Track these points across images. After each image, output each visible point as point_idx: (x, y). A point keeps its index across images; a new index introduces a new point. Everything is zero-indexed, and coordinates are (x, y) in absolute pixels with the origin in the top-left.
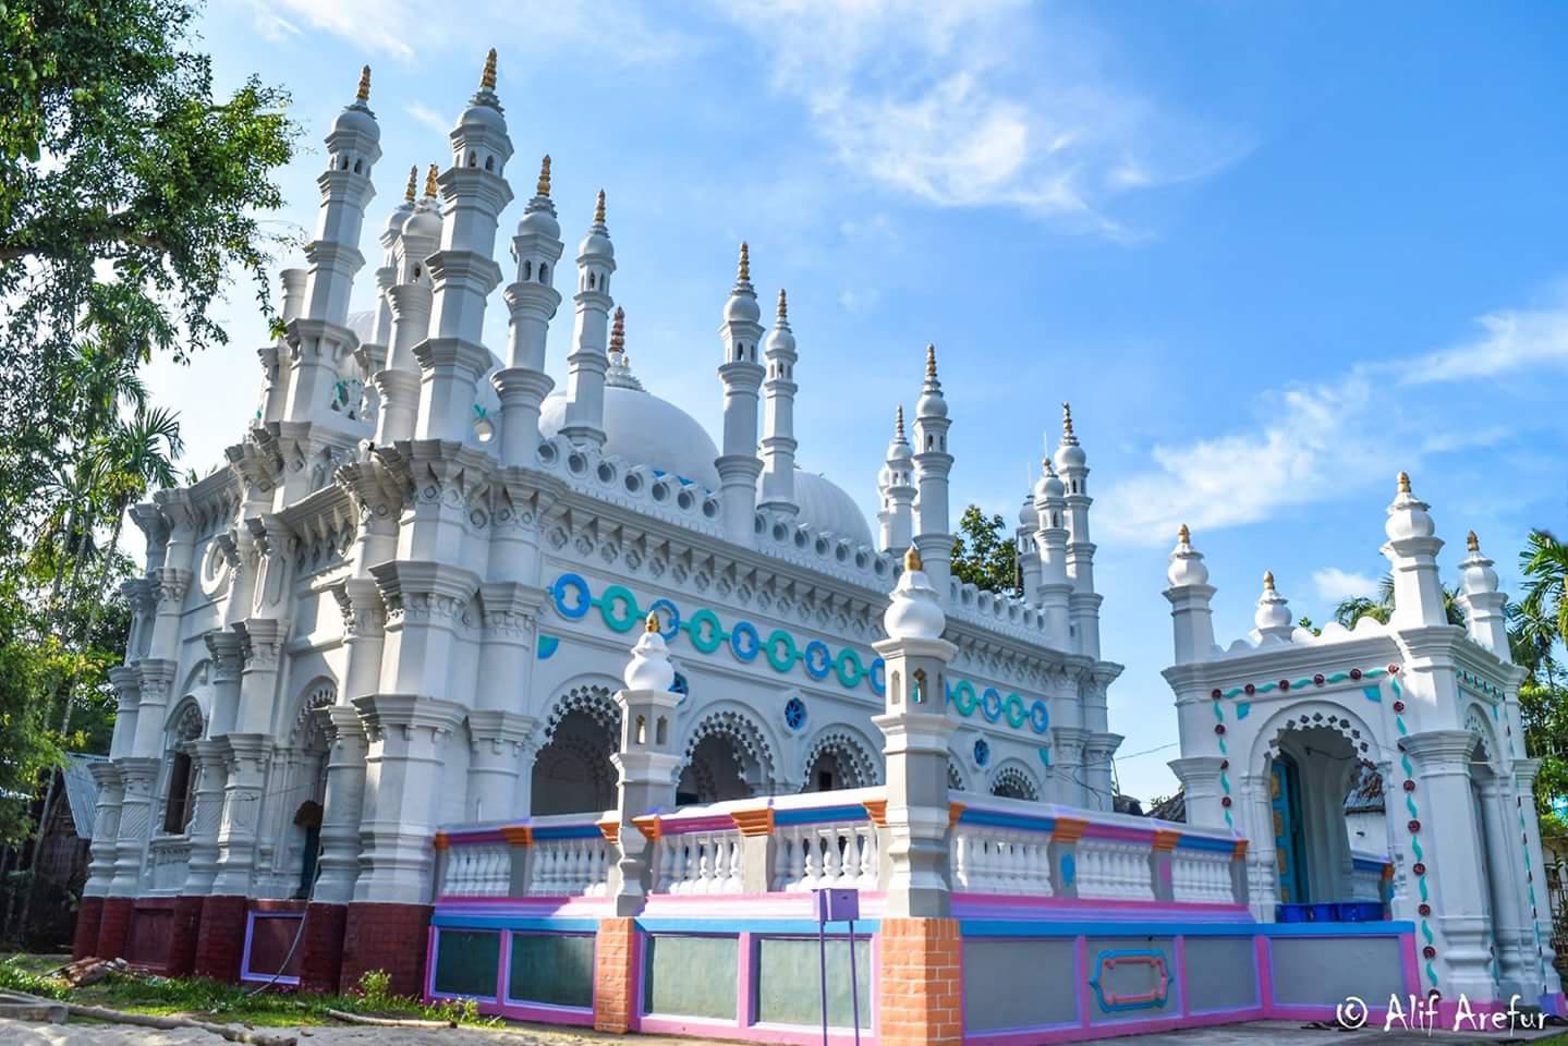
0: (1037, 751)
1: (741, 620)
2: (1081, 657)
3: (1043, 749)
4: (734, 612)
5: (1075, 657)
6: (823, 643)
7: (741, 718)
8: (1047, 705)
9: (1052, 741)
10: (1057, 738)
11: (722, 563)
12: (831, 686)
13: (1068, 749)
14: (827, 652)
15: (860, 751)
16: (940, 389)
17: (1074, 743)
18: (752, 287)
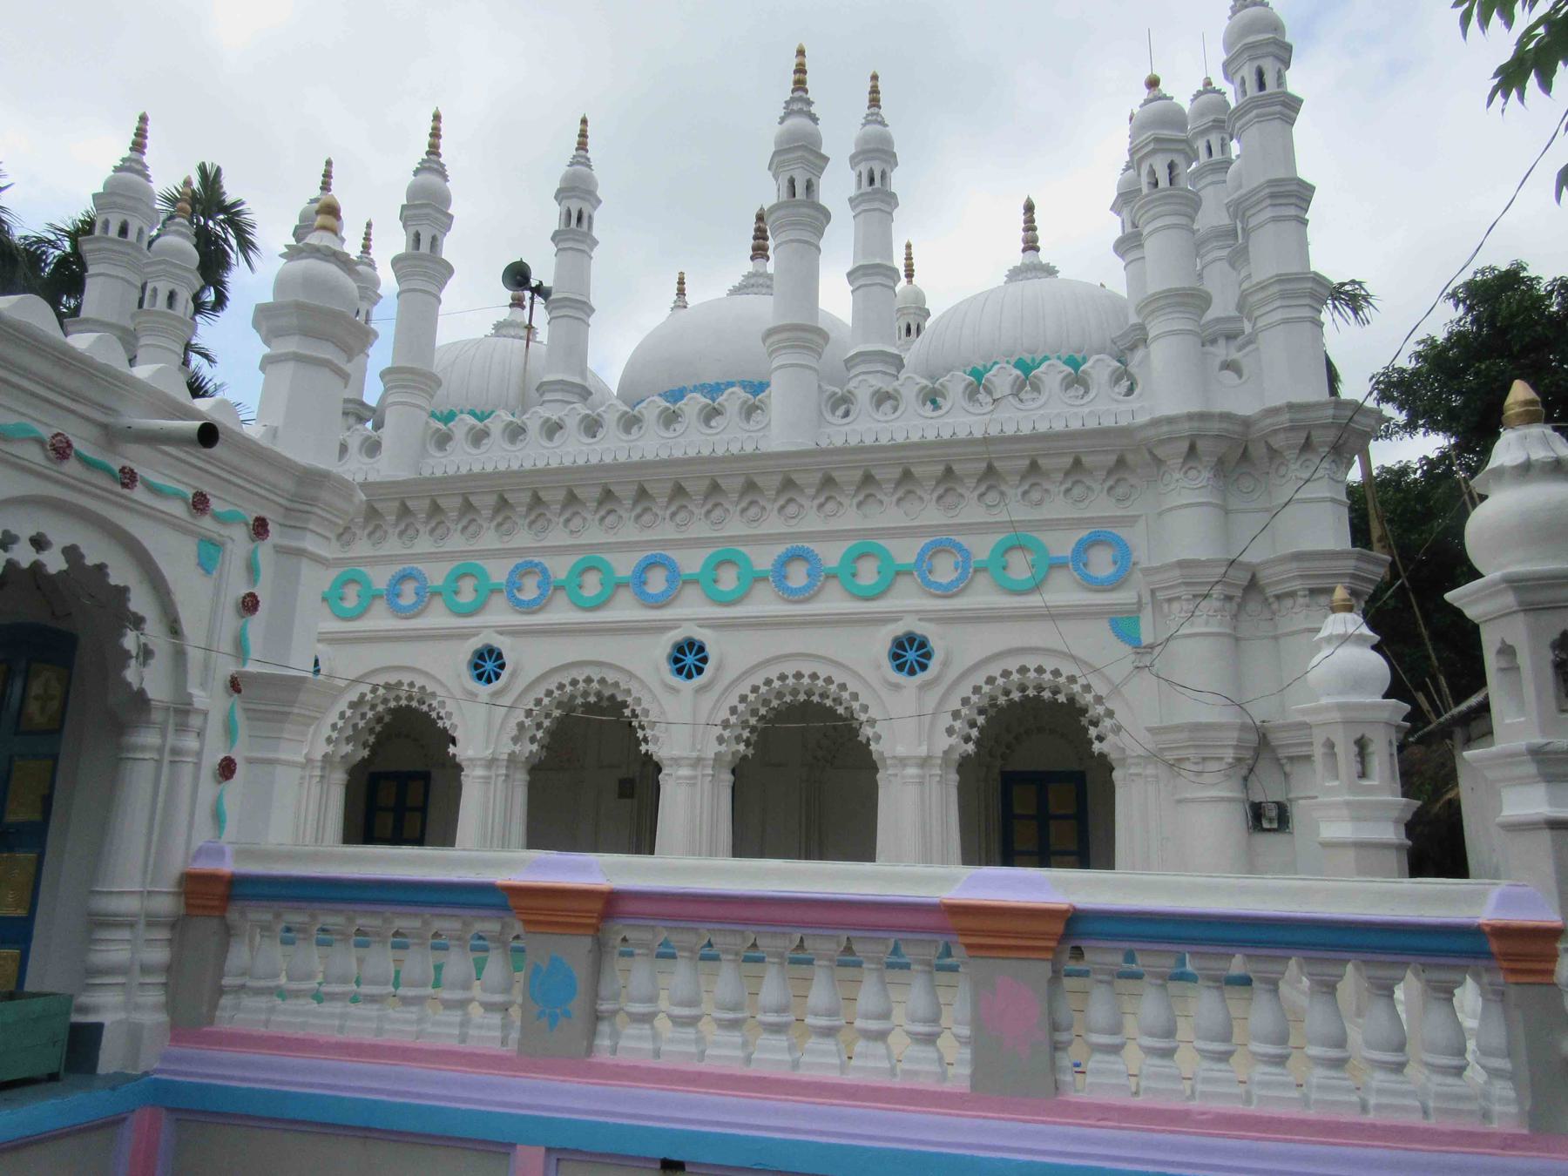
0: (1102, 629)
1: (400, 567)
2: (1170, 420)
3: (1123, 624)
4: (389, 559)
5: (1156, 423)
6: (536, 560)
7: (412, 685)
8: (1135, 537)
9: (1146, 598)
10: (1153, 592)
11: (420, 506)
12: (561, 613)
13: (1176, 606)
14: (544, 571)
15: (628, 692)
16: (813, 109)
17: (1182, 591)
18: (443, 166)
